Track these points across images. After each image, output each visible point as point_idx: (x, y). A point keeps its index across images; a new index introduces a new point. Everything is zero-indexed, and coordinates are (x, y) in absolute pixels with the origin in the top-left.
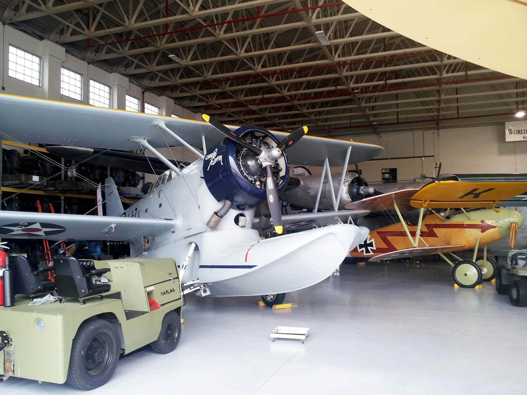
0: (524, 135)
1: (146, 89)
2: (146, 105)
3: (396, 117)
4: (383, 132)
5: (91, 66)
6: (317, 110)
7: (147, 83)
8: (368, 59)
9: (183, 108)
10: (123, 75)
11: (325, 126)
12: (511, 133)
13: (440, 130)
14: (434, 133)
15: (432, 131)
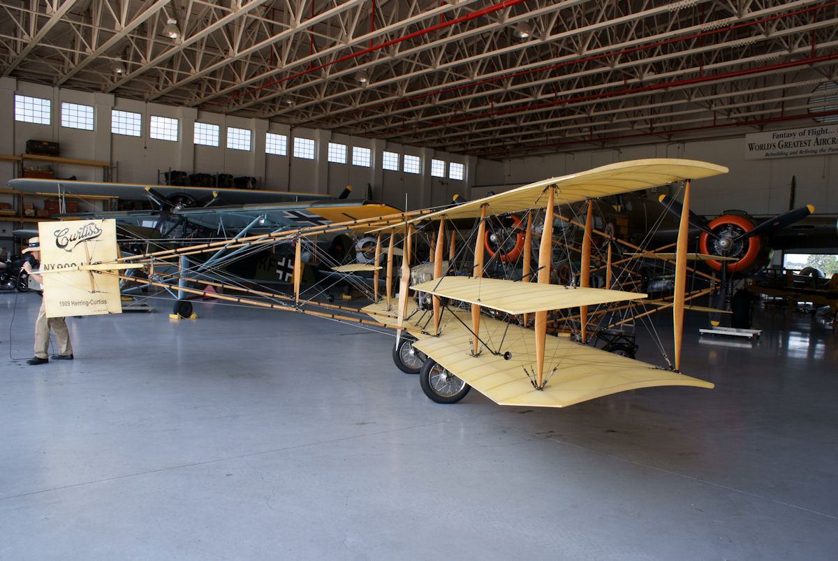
0: (767, 151)
1: (296, 125)
2: (296, 140)
3: (713, 118)
4: (623, 146)
5: (228, 116)
6: (550, 120)
7: (294, 120)
8: (518, 72)
9: (350, 135)
10: (261, 118)
11: (539, 141)
12: (751, 148)
13: (686, 144)
14: (679, 148)
15: (678, 145)
